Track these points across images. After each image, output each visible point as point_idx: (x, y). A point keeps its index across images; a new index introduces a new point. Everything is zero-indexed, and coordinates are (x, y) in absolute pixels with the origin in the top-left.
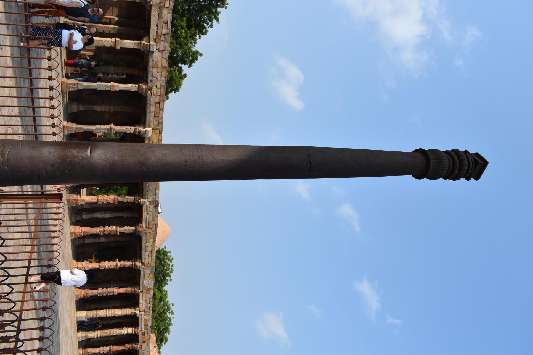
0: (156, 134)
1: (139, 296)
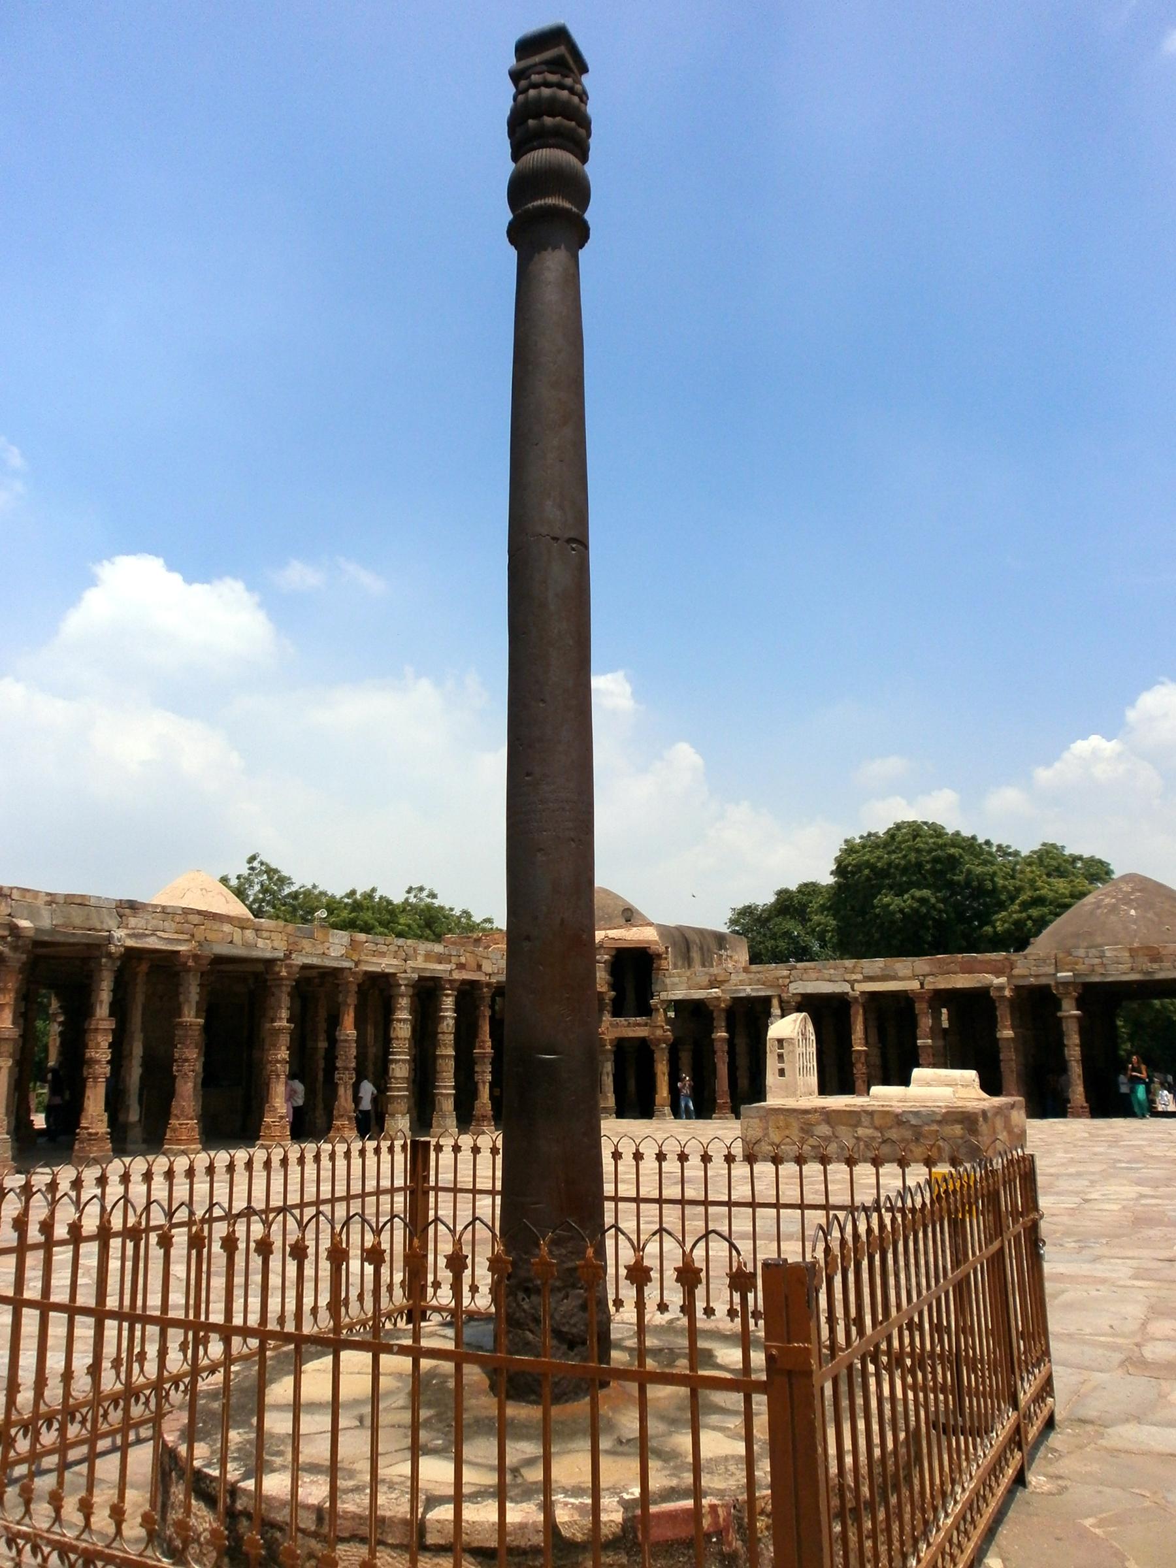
1: (366, 973)
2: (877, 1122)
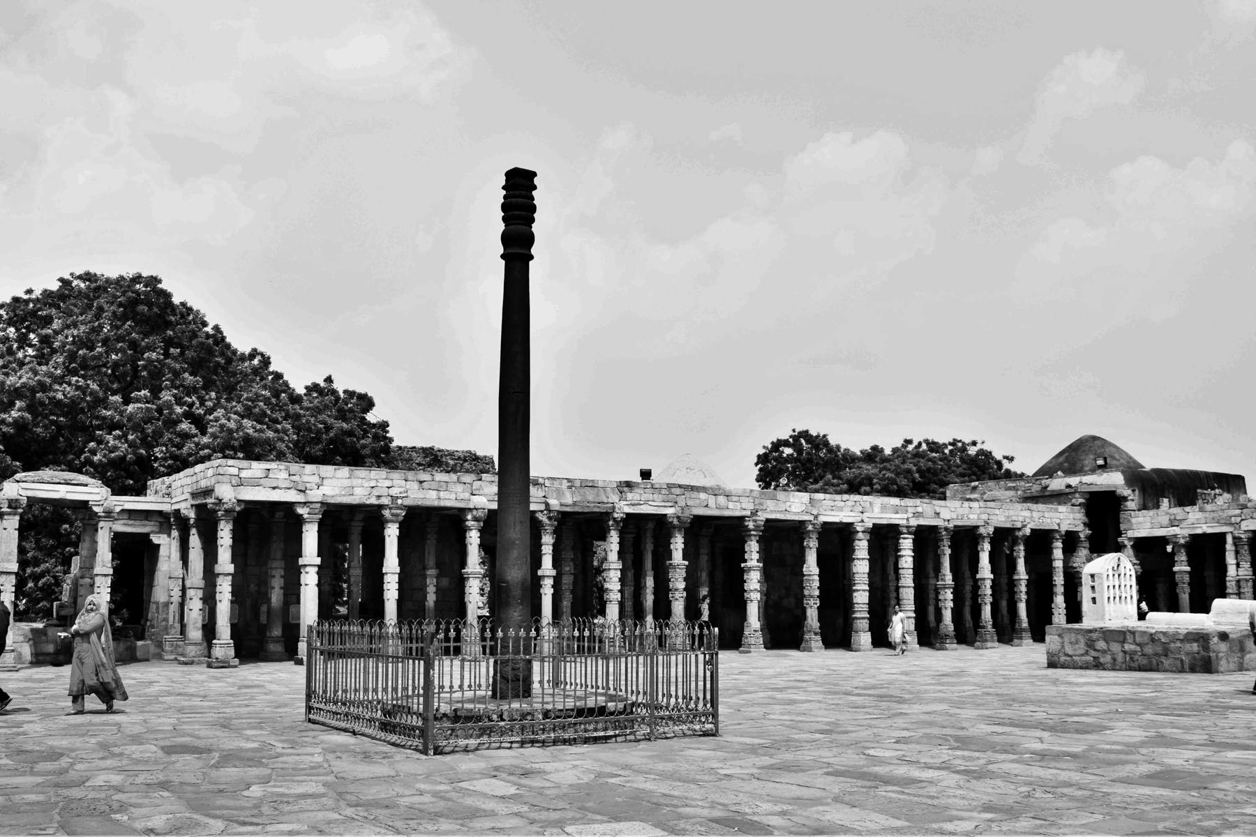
1: (825, 523)
2: (1138, 639)
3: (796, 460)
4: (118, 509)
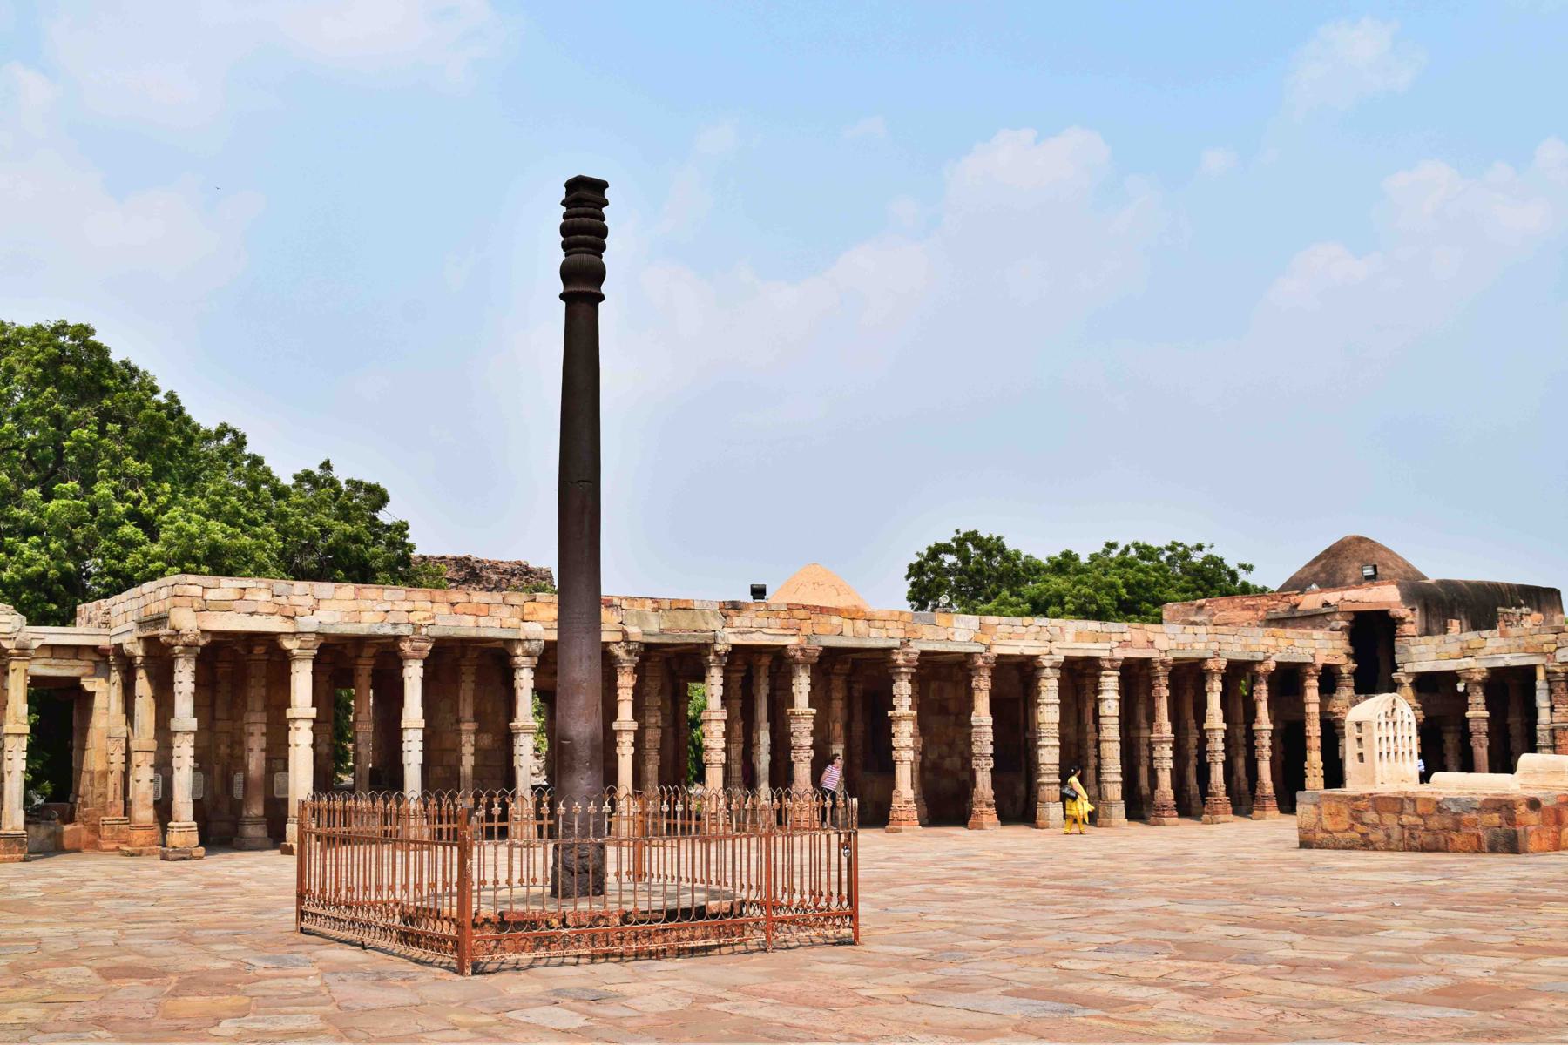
0: (534, 611)
1: (1000, 656)
2: (1420, 809)
3: (962, 572)
4: (36, 644)
